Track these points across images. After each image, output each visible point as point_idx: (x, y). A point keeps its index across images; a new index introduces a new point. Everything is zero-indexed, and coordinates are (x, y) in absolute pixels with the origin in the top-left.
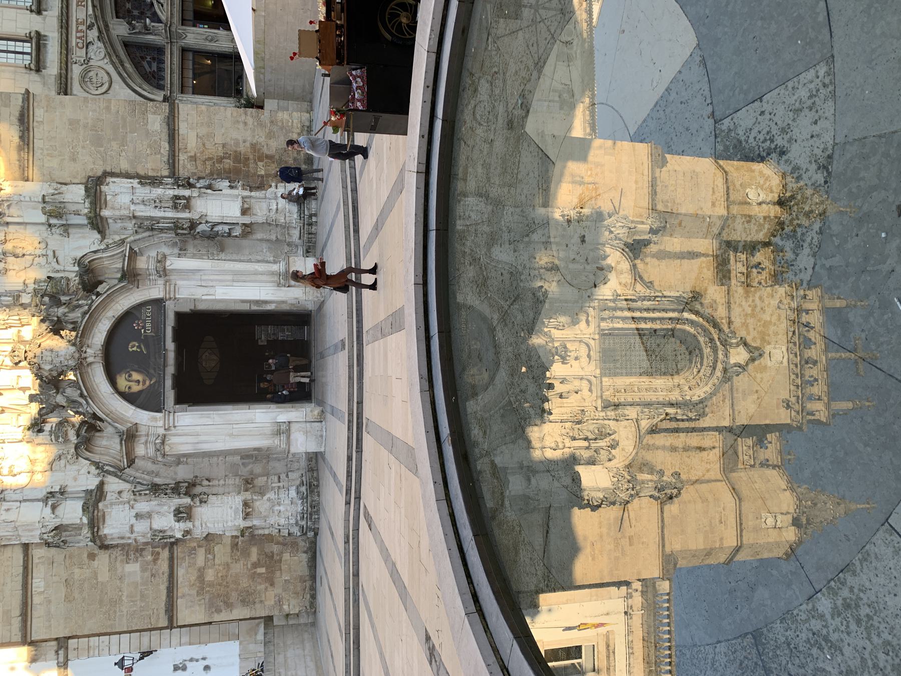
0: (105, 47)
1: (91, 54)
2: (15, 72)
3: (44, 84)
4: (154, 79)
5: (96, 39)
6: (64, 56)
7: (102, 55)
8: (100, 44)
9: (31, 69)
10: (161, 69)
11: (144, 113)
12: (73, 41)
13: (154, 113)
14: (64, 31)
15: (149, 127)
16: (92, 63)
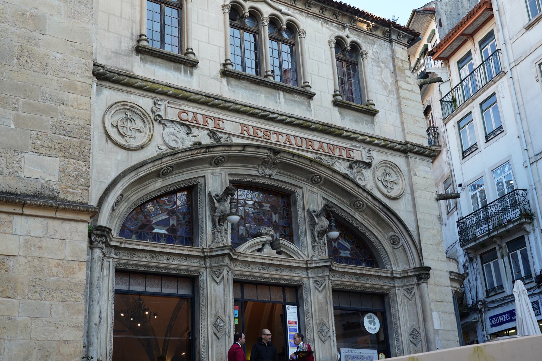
0: (185, 151)
1: (171, 129)
2: (133, 22)
3: (117, 53)
4: (137, 224)
5: (196, 140)
6: (165, 89)
7: (173, 144)
8: (188, 143)
9: (138, 41)
10: (157, 238)
11: (63, 151)
12: (191, 108)
13: (63, 171)
14: (204, 99)
15: (30, 156)
16: (158, 127)
